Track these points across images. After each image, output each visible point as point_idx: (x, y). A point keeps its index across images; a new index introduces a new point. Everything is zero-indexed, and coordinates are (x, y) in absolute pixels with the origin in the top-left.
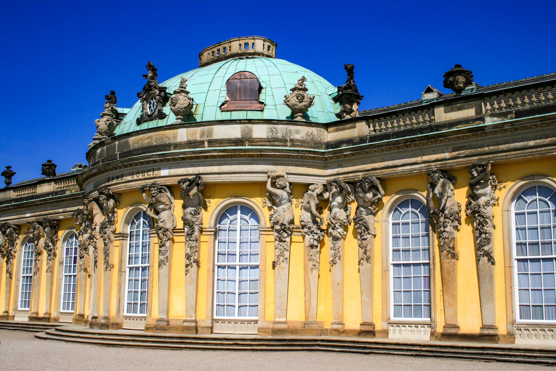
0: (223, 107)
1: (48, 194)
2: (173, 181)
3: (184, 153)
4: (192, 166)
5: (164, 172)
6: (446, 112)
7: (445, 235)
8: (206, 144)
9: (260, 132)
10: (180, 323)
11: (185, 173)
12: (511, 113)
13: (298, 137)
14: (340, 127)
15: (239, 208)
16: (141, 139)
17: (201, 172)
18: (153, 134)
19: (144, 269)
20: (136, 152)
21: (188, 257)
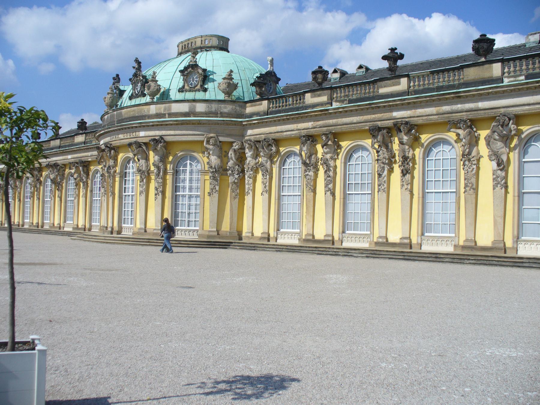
0: (181, 90)
1: (81, 143)
2: (146, 140)
3: (152, 122)
4: (158, 130)
5: (142, 134)
6: (312, 97)
7: (308, 177)
8: (167, 115)
9: (200, 108)
10: (152, 231)
11: (154, 135)
12: (346, 100)
13: (226, 110)
14: (253, 103)
15: (189, 157)
16: (129, 112)
17: (164, 134)
18: (136, 108)
19: (132, 196)
20: (126, 120)
21: (156, 189)
